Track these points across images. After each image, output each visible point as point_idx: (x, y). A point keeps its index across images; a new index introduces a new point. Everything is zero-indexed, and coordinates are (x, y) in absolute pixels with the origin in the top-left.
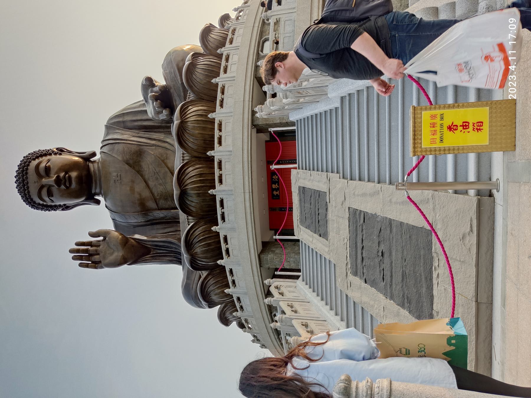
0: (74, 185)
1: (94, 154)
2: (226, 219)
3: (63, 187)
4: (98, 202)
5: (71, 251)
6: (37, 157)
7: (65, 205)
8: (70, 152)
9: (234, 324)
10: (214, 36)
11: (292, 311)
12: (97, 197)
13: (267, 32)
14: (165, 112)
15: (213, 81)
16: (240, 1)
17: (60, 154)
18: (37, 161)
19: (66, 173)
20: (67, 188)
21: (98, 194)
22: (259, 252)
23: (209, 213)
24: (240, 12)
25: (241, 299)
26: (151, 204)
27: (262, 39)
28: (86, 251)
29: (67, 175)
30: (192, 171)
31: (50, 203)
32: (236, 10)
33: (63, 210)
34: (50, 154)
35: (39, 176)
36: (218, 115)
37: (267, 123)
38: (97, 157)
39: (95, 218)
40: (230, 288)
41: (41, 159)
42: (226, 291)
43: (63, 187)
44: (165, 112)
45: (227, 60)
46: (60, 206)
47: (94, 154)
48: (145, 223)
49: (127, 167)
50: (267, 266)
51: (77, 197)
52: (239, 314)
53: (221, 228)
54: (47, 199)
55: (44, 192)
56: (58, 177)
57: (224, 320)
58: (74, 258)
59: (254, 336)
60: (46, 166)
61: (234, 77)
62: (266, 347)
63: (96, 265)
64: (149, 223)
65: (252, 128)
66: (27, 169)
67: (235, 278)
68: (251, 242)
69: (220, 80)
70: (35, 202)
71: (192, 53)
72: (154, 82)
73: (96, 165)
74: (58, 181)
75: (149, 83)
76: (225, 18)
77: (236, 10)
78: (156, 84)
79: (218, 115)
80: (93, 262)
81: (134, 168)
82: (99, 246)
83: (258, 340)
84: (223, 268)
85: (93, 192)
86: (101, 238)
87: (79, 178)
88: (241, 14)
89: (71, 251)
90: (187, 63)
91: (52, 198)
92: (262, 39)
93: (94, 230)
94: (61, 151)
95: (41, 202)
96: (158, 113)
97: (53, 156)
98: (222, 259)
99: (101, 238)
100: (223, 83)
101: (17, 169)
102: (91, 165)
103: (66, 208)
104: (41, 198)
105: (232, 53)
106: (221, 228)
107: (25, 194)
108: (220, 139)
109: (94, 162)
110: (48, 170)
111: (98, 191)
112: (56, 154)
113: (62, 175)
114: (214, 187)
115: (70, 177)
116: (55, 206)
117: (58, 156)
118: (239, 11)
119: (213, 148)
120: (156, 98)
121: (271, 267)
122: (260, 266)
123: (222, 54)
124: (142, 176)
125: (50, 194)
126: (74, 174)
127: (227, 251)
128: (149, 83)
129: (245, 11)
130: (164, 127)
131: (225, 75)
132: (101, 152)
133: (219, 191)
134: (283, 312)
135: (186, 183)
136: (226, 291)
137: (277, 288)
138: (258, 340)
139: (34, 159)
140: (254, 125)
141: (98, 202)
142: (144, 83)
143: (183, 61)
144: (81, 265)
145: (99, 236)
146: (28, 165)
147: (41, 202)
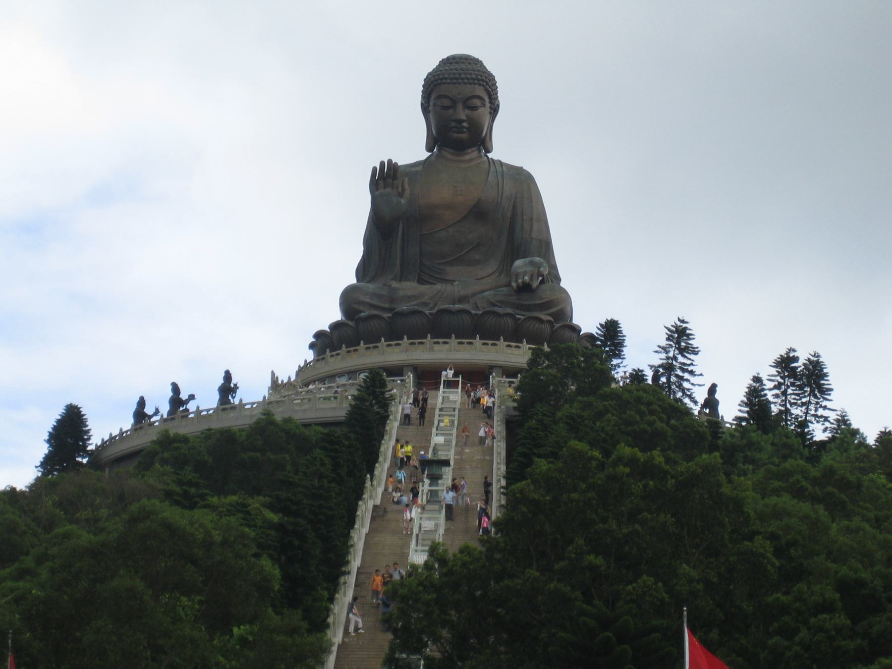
3: (453, 124)
8: (493, 121)
17: (490, 113)
33: (422, 104)
34: (491, 102)
36: (502, 343)
43: (453, 124)
46: (429, 106)
47: (488, 151)
51: (437, 133)
53: (428, 340)
55: (446, 102)
58: (382, 164)
70: (435, 86)
73: (475, 154)
79: (502, 343)
82: (393, 188)
89: (390, 161)
94: (494, 110)
96: (517, 275)
104: (439, 97)
107: (446, 79)
112: (491, 108)
113: (465, 124)
119: (481, 339)
125: (446, 108)
141: (429, 148)
144: (375, 169)
146: (480, 85)
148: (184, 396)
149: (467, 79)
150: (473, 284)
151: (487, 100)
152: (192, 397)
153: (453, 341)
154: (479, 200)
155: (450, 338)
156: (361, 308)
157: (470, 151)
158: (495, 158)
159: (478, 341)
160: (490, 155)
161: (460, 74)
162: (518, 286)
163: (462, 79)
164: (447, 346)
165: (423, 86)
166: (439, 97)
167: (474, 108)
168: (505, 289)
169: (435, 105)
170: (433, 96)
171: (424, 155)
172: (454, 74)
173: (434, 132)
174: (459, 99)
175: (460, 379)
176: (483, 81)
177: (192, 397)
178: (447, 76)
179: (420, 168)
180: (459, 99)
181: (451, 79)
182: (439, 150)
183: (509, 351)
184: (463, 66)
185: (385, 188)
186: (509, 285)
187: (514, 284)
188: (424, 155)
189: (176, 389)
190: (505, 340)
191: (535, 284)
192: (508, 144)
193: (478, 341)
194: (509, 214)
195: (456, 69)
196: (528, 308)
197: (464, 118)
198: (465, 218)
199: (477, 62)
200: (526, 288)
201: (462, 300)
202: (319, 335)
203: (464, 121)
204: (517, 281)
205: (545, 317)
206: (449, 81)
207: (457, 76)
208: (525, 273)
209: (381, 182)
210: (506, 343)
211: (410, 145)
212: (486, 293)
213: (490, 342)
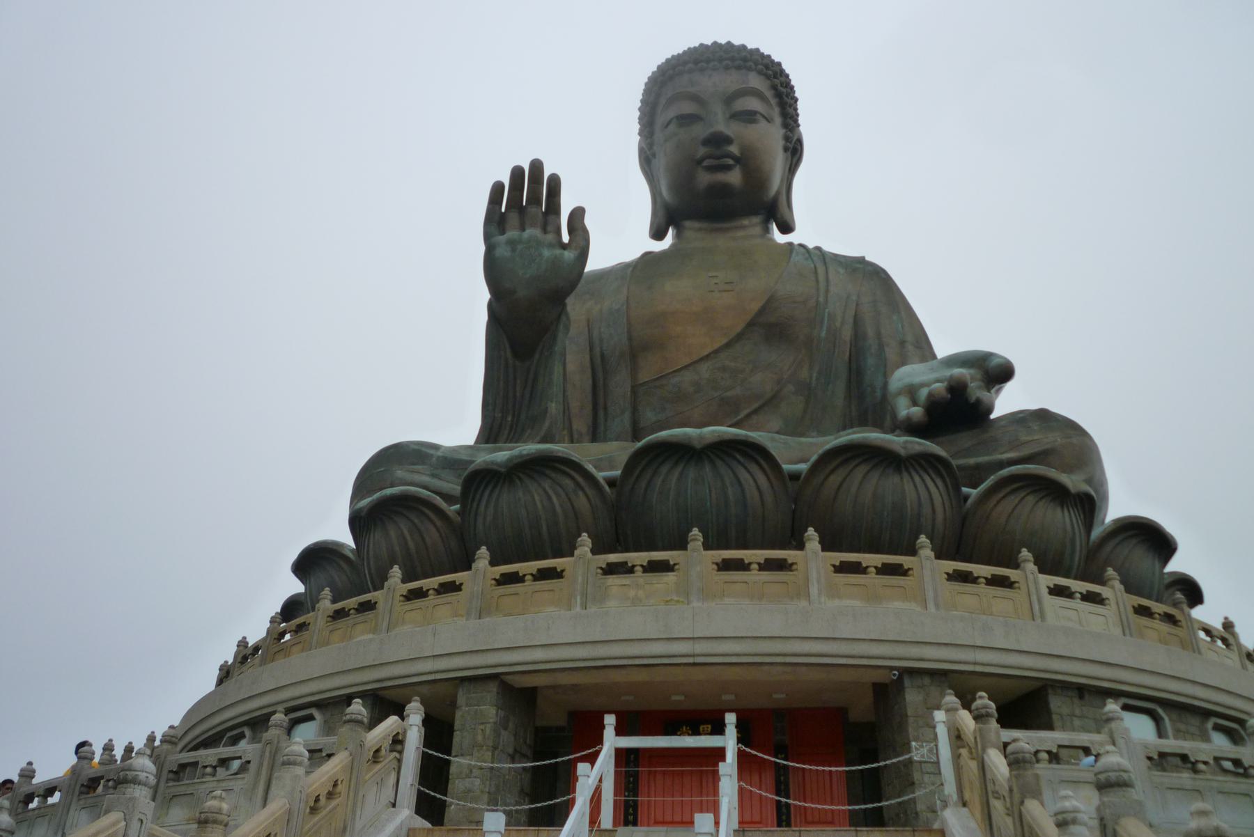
0: (704, 179)
1: (786, 228)
2: (613, 580)
3: (702, 151)
4: (658, 234)
5: (537, 166)
6: (779, 95)
7: (654, 155)
9: (298, 587)
10: (1140, 559)
11: (317, 800)
12: (670, 231)
13: (1182, 727)
14: (917, 412)
15: (1025, 553)
16: (1253, 637)
17: (786, 149)
18: (769, 94)
19: (738, 160)
20: (699, 162)
21: (678, 236)
22: (509, 679)
23: (632, 528)
24: (1224, 640)
25: (370, 615)
26: (649, 370)
27: (1160, 711)
28: (534, 198)
29: (731, 162)
30: (753, 480)
31: (661, 120)
32: (1228, 625)
33: (641, 151)
35: (729, 99)
37: (911, 720)
38: (779, 238)
39: (618, 223)
40: (404, 581)
41: (773, 101)
42: (396, 572)
44: (917, 412)
45: (1090, 598)
47: (786, 228)
48: (597, 350)
49: (755, 306)
50: (461, 699)
52: (326, 605)
53: (583, 559)
54: (672, 113)
55: (687, 108)
56: (729, 141)
57: (313, 561)
58: (517, 173)
59: (256, 648)
60: (754, 113)
61: (1043, 617)
62: (220, 682)
63: (495, 222)
64: (598, 361)
65: (892, 668)
66: (750, 69)
67: (432, 599)
68: (539, 655)
69: (1029, 574)
71: (1093, 493)
72: (997, 387)
73: (758, 230)
74: (717, 141)
75: (999, 373)
76: (1192, 592)
77: (1228, 625)
78: (993, 391)
80: (503, 217)
81: (751, 324)
82: (545, 231)
83: (245, 658)
84: (466, 563)
85: (688, 224)
86: (566, 238)
87: (723, 190)
88: (1219, 643)
89: (537, 166)
90: (1068, 480)
91: (672, 127)
92: (1160, 711)
93: (588, 222)
94: (794, 151)
95: (663, 101)
96: (911, 392)
97: (782, 131)
98: (493, 563)
99: (566, 238)
100: (1023, 585)
101: (749, 47)
102: (756, 220)
103: (647, 160)
105: (1109, 611)
106: (583, 559)
107: (685, 63)
108: (856, 568)
109: (767, 230)
110: (749, 117)
111: (688, 234)
113: (734, 149)
114: (707, 546)
115: (727, 168)
117: (781, 143)
118: (1226, 635)
119: (827, 546)
120: (957, 389)
121: (458, 714)
122: (463, 680)
123: (1102, 582)
124: (728, 345)
125: (686, 120)
126: (734, 177)
127: (513, 578)
128: (1000, 373)
129: (1227, 653)
130: (872, 410)
131: (1045, 591)
132: (791, 244)
133: (698, 559)
134: (318, 755)
135: (719, 463)
136: (396, 572)
137: (398, 742)
138: (245, 658)
139: (774, 87)
140: (900, 677)
141: (658, 234)
142: (995, 362)
143: (1069, 469)
144: (497, 189)
145: (570, 232)
147: (663, 101)
151: (778, 120)
153: (698, 559)
154: (771, 300)
155: (681, 544)
157: (746, 222)
159: (813, 557)
164: (670, 577)
166: (671, 101)
167: (749, 117)
175: (729, 741)
183: (968, 595)
185: (523, 230)
193: (813, 557)
194: (847, 333)
198: (739, 337)
209: (514, 219)
213: (872, 560)
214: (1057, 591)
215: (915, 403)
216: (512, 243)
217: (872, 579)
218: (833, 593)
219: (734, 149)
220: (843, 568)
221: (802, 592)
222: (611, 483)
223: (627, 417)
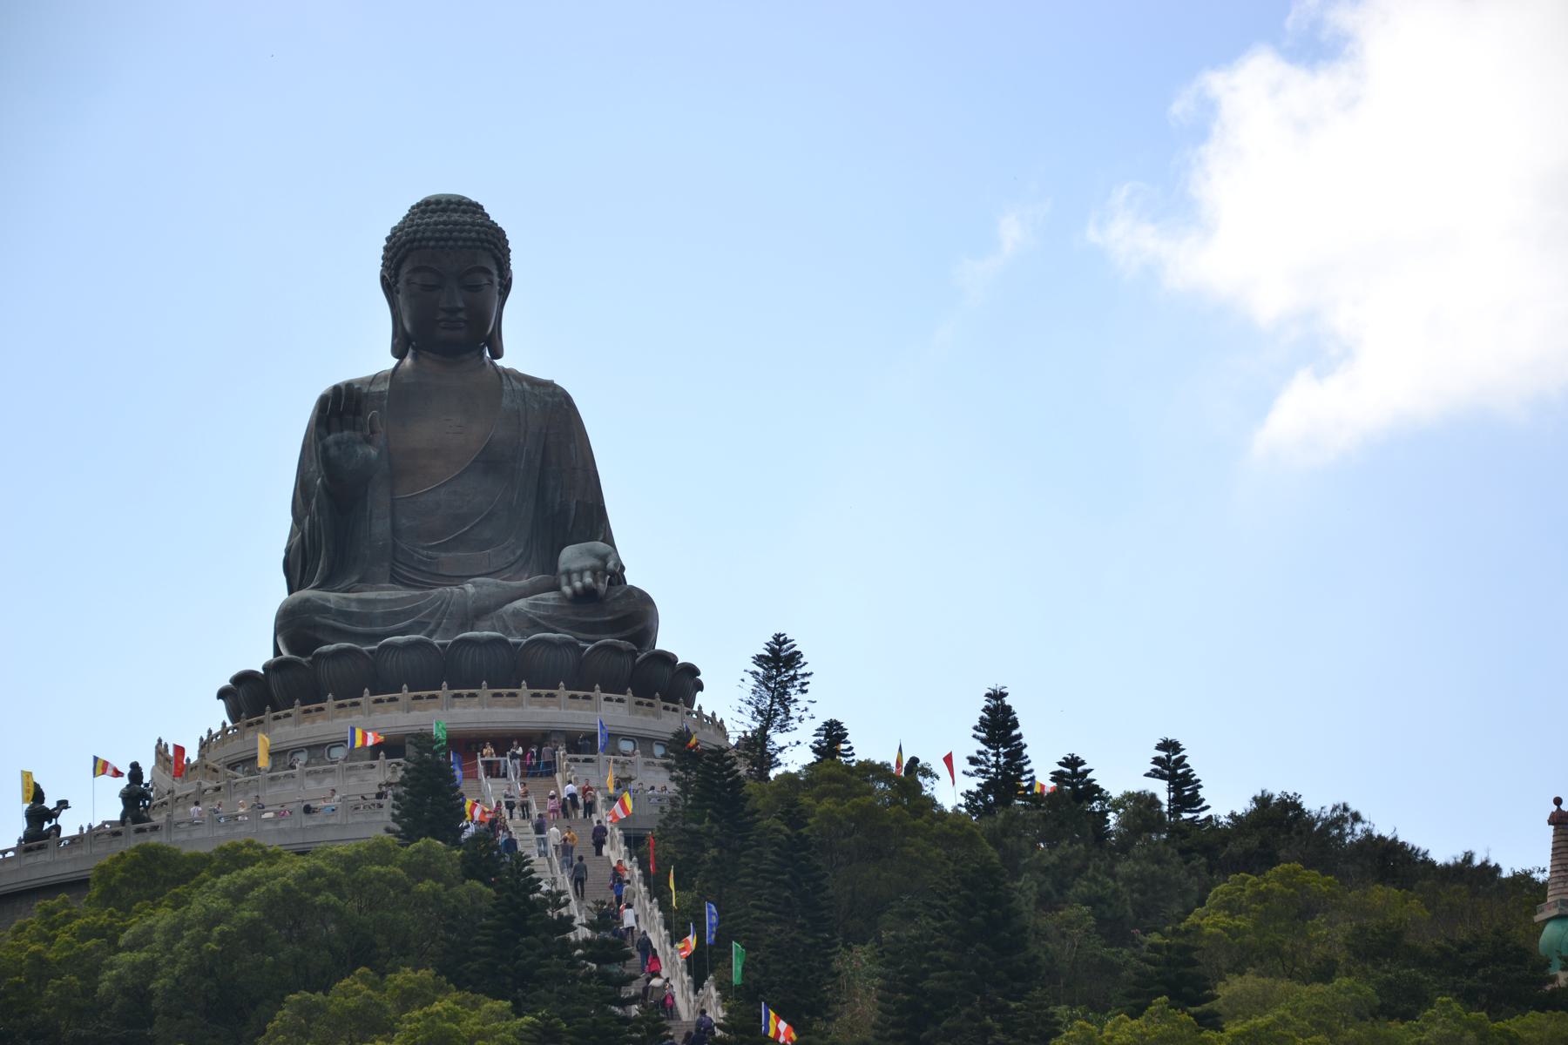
3: (442, 316)
33: (383, 278)
36: (562, 692)
43: (442, 316)
47: (497, 353)
53: (444, 692)
79: (562, 692)
96: (568, 573)
103: (390, 285)
107: (429, 239)
108: (538, 695)
113: (462, 315)
116: (397, 275)
141: (398, 352)
148: (50, 803)
149: (465, 240)
150: (504, 597)
151: (495, 272)
152: (63, 804)
156: (319, 636)
158: (507, 366)
159: (524, 691)
160: (498, 362)
161: (450, 232)
162: (575, 592)
163: (456, 240)
165: (386, 249)
168: (552, 595)
169: (408, 282)
170: (405, 270)
171: (390, 363)
172: (442, 231)
173: (407, 326)
174: (447, 267)
176: (489, 242)
177: (63, 804)
178: (428, 234)
179: (385, 387)
180: (447, 267)
181: (437, 240)
182: (415, 357)
184: (455, 217)
186: (557, 588)
187: (567, 590)
188: (390, 363)
189: (38, 795)
190: (567, 688)
191: (602, 587)
192: (529, 342)
193: (524, 691)
195: (444, 223)
196: (594, 629)
197: (461, 305)
199: (476, 208)
200: (587, 596)
201: (477, 614)
202: (244, 680)
203: (460, 310)
204: (570, 583)
205: (624, 644)
206: (432, 243)
207: (445, 234)
208: (581, 572)
210: (571, 692)
211: (367, 348)
212: (520, 604)
213: (544, 692)
214: (608, 699)
215: (570, 583)
216: (338, 443)
217: (543, 699)
218: (531, 704)
219: (462, 315)
220: (535, 695)
221: (520, 705)
222: (443, 646)
223: (388, 520)
